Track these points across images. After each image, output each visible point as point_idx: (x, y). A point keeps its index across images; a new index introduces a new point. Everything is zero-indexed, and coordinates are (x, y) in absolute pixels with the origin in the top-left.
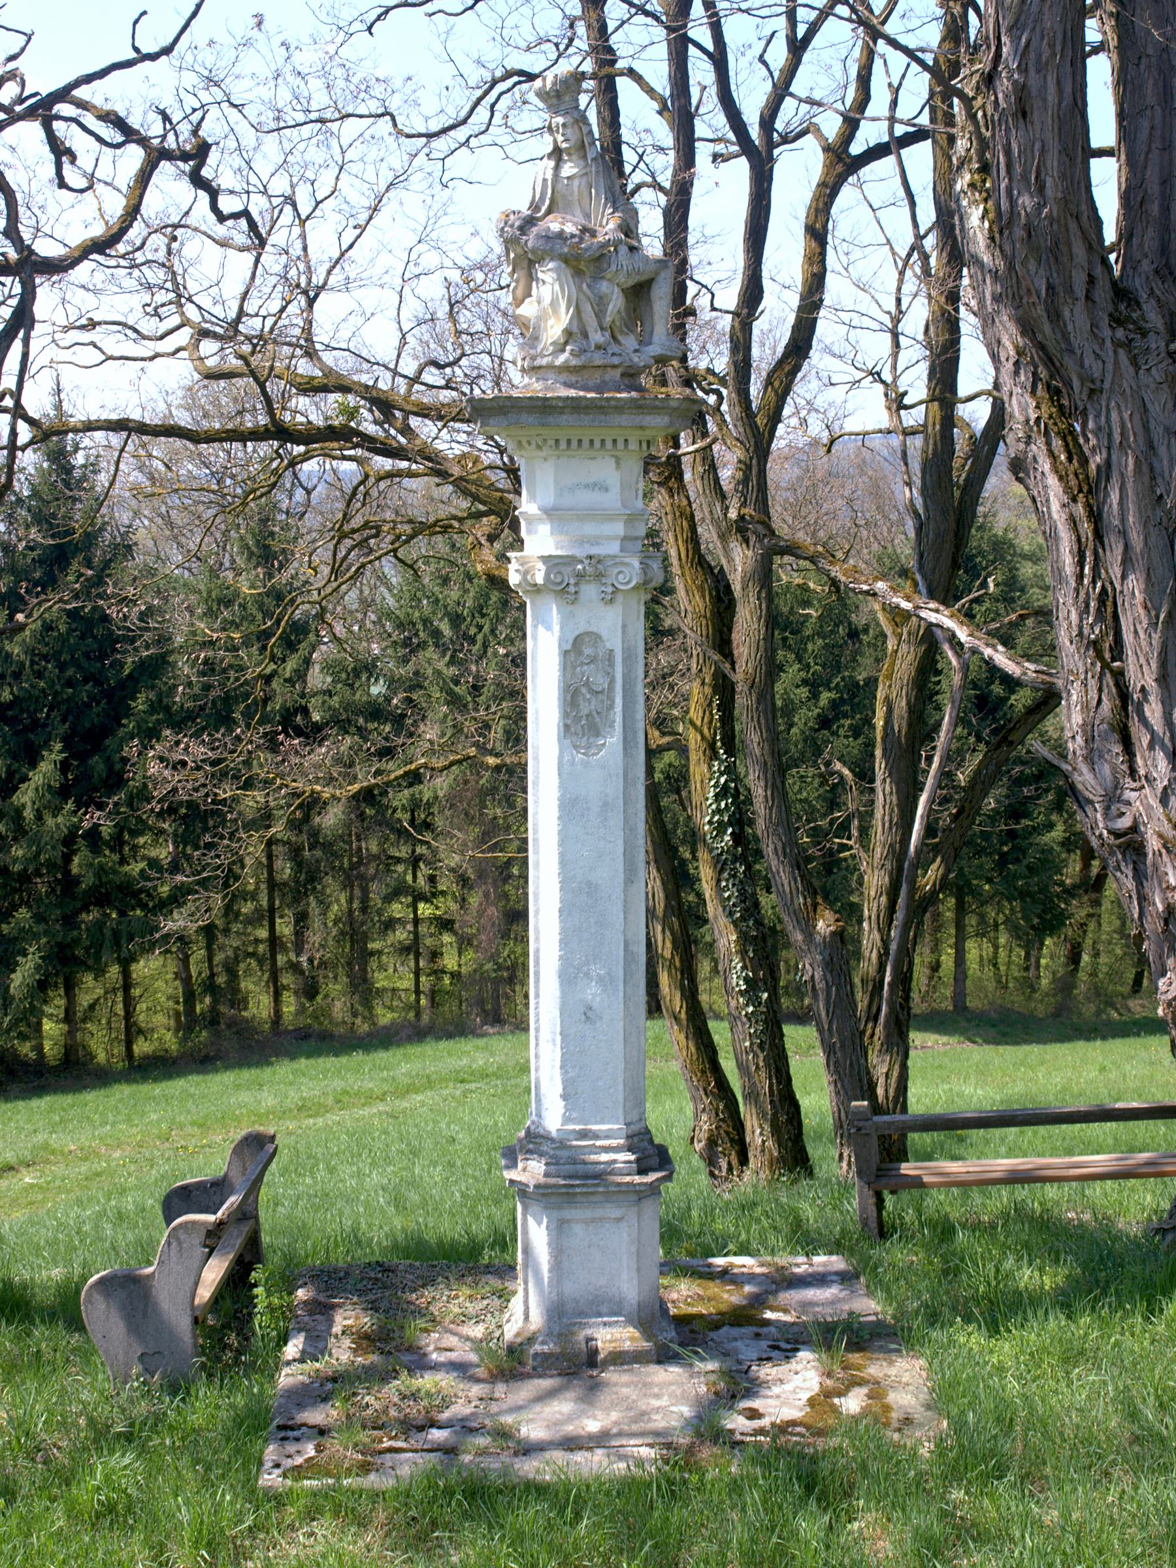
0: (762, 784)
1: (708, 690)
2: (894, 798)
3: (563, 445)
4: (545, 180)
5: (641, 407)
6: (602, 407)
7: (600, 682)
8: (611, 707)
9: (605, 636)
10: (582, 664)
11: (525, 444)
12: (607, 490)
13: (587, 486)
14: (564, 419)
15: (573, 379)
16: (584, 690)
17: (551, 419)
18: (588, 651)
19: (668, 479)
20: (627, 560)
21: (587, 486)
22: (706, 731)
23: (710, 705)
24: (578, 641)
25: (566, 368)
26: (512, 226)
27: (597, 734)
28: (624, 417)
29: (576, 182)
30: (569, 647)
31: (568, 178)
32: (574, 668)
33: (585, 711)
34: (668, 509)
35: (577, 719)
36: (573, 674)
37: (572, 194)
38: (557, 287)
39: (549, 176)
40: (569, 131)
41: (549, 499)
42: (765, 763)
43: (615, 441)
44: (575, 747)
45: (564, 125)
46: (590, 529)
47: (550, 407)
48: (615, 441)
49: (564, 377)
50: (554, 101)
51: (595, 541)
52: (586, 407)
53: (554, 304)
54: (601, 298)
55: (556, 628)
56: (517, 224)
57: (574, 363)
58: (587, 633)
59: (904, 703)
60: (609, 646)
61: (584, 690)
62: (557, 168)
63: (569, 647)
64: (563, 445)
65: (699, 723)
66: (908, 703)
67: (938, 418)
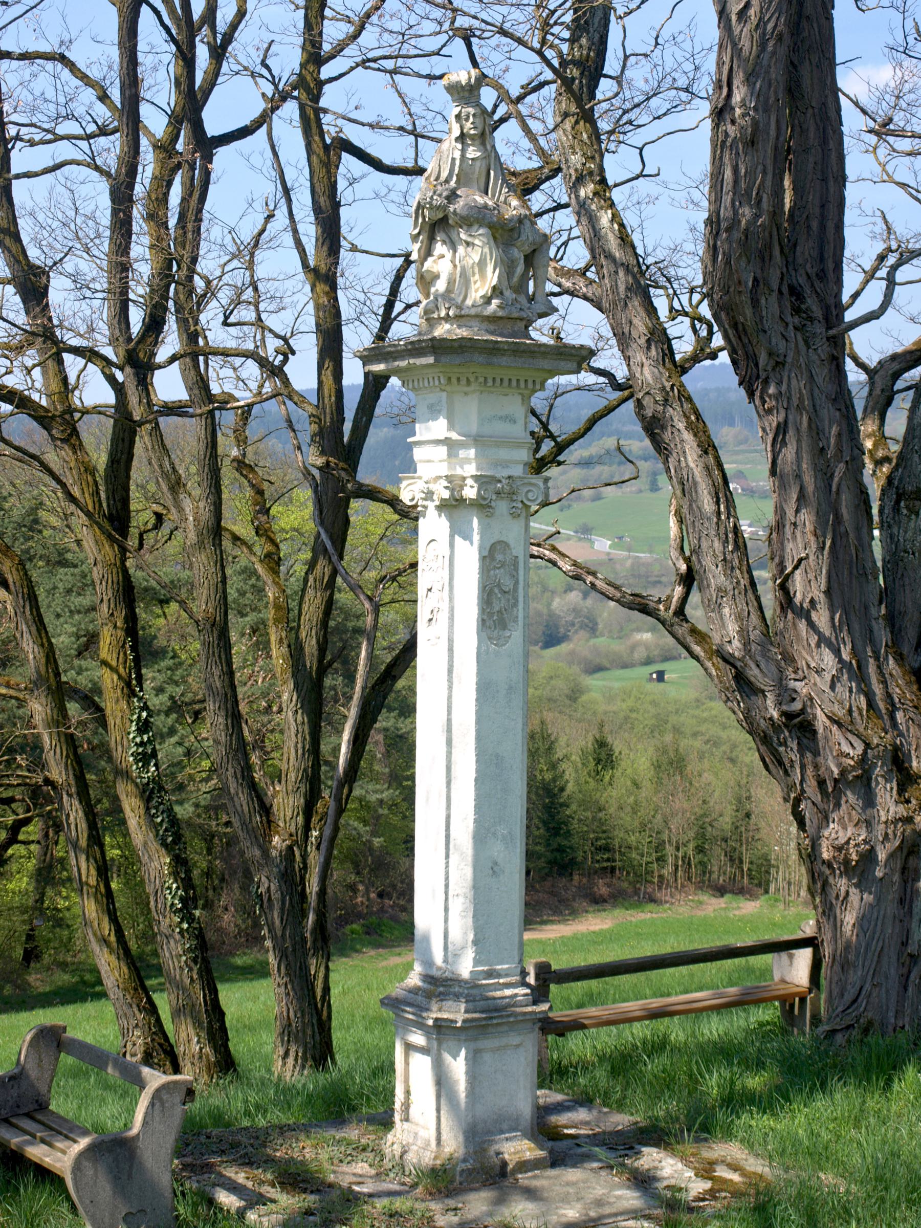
0: (223, 713)
1: (121, 633)
2: (306, 728)
3: (490, 383)
4: (453, 159)
5: (561, 354)
6: (534, 352)
7: (508, 583)
8: (516, 604)
9: (512, 543)
10: (495, 568)
11: (454, 380)
12: (515, 422)
13: (501, 418)
14: (504, 360)
15: (492, 327)
16: (496, 591)
17: (495, 360)
18: (499, 557)
19: (71, 435)
20: (533, 481)
21: (501, 418)
22: (121, 670)
23: (123, 646)
24: (493, 549)
25: (492, 319)
26: (440, 195)
27: (504, 627)
28: (546, 361)
29: (478, 164)
30: (486, 554)
31: (473, 159)
32: (489, 571)
33: (497, 608)
34: (72, 465)
35: (491, 615)
36: (488, 576)
37: (473, 173)
38: (486, 250)
39: (457, 154)
40: (477, 121)
41: (474, 428)
42: (226, 695)
43: (518, 380)
44: (490, 638)
45: (474, 115)
46: (504, 454)
47: (498, 349)
48: (518, 380)
49: (485, 325)
50: (466, 94)
51: (505, 464)
52: (523, 352)
53: (482, 264)
54: (512, 261)
55: (476, 538)
56: (445, 194)
57: (500, 314)
58: (499, 542)
59: (314, 642)
60: (515, 553)
61: (496, 591)
62: (463, 151)
63: (486, 554)
64: (490, 383)
65: (114, 663)
66: (318, 642)
67: (333, 390)
